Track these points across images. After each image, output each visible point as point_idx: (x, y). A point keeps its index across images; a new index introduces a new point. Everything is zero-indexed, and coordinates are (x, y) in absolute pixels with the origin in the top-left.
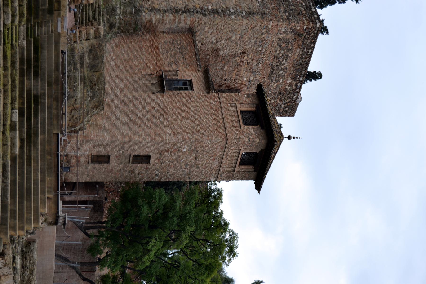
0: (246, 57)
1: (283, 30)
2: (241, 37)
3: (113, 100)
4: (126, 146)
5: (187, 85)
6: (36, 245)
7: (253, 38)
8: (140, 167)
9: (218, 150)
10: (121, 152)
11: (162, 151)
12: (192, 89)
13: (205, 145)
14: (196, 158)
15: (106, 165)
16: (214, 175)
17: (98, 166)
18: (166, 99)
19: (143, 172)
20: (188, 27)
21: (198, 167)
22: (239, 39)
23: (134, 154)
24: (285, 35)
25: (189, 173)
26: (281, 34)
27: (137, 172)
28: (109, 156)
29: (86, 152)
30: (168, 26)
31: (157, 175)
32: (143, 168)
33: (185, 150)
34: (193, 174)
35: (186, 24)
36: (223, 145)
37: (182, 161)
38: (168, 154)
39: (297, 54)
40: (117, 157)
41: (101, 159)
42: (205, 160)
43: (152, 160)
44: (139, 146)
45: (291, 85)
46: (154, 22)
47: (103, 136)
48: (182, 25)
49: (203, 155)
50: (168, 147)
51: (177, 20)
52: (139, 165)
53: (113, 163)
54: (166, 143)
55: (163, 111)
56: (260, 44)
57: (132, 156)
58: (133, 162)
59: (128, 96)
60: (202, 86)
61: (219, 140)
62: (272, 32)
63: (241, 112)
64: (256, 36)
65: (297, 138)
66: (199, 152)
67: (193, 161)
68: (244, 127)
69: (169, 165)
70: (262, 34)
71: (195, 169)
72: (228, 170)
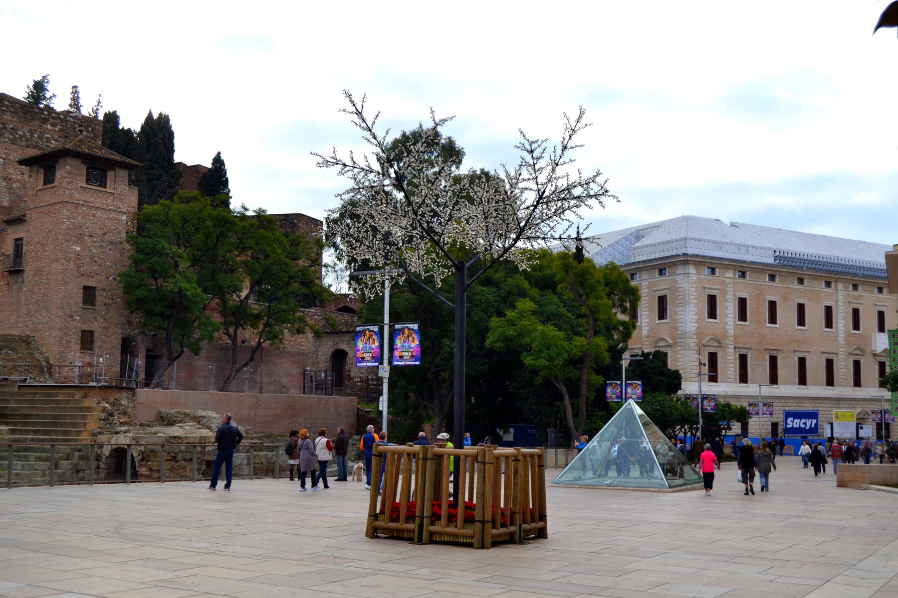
0: (13, 176)
3: (27, 326)
4: (68, 313)
5: (18, 242)
6: (163, 410)
8: (100, 298)
9: (80, 211)
12: (21, 239)
15: (96, 334)
17: (97, 343)
18: (29, 267)
19: (109, 294)
21: (105, 234)
23: (81, 305)
25: (113, 243)
28: (83, 331)
29: (77, 357)
31: (114, 279)
33: (78, 249)
34: (115, 238)
36: (72, 208)
39: (10, 118)
41: (87, 340)
43: (91, 284)
44: (70, 298)
45: (54, 125)
47: (55, 337)
50: (73, 266)
52: (98, 298)
53: (95, 326)
55: (38, 271)
58: (94, 305)
59: (24, 310)
60: (20, 228)
63: (45, 184)
68: (56, 183)
71: (108, 237)
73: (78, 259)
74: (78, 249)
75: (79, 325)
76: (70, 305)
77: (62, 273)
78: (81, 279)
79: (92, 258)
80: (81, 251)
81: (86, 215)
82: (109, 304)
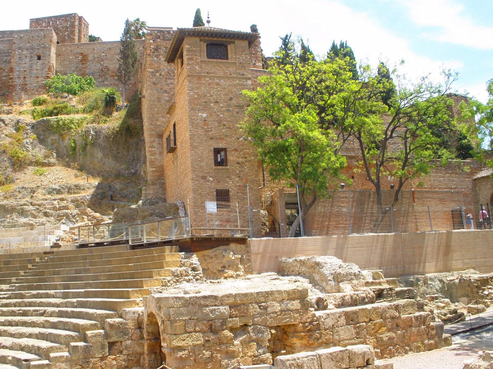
1: (156, 59)
2: (166, 92)
4: (201, 174)
7: (167, 81)
9: (203, 82)
10: (211, 179)
11: (207, 137)
13: (196, 96)
14: (217, 102)
16: (241, 82)
20: (158, 139)
21: (231, 99)
22: (168, 93)
23: (213, 166)
24: (161, 56)
26: (160, 59)
27: (240, 160)
28: (217, 191)
30: (157, 156)
32: (236, 154)
33: (205, 115)
35: (154, 141)
37: (222, 116)
38: (211, 131)
40: (219, 182)
42: (219, 93)
43: (221, 146)
46: (154, 169)
48: (155, 144)
49: (212, 96)
50: (200, 132)
51: (150, 149)
54: (195, 135)
56: (172, 75)
57: (216, 167)
61: (187, 83)
62: (159, 67)
64: (164, 80)
65: (208, 15)
66: (206, 101)
67: (221, 105)
69: (229, 128)
70: (161, 75)
71: (234, 102)
72: (235, 69)
73: (205, 124)
74: (205, 115)
75: (212, 185)
76: (201, 167)
77: (191, 139)
78: (211, 142)
79: (220, 122)
80: (207, 117)
81: (209, 84)
82: (243, 163)
